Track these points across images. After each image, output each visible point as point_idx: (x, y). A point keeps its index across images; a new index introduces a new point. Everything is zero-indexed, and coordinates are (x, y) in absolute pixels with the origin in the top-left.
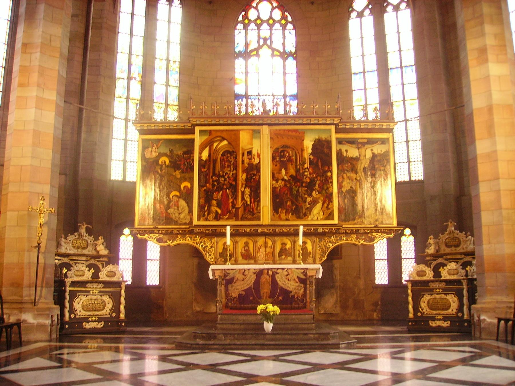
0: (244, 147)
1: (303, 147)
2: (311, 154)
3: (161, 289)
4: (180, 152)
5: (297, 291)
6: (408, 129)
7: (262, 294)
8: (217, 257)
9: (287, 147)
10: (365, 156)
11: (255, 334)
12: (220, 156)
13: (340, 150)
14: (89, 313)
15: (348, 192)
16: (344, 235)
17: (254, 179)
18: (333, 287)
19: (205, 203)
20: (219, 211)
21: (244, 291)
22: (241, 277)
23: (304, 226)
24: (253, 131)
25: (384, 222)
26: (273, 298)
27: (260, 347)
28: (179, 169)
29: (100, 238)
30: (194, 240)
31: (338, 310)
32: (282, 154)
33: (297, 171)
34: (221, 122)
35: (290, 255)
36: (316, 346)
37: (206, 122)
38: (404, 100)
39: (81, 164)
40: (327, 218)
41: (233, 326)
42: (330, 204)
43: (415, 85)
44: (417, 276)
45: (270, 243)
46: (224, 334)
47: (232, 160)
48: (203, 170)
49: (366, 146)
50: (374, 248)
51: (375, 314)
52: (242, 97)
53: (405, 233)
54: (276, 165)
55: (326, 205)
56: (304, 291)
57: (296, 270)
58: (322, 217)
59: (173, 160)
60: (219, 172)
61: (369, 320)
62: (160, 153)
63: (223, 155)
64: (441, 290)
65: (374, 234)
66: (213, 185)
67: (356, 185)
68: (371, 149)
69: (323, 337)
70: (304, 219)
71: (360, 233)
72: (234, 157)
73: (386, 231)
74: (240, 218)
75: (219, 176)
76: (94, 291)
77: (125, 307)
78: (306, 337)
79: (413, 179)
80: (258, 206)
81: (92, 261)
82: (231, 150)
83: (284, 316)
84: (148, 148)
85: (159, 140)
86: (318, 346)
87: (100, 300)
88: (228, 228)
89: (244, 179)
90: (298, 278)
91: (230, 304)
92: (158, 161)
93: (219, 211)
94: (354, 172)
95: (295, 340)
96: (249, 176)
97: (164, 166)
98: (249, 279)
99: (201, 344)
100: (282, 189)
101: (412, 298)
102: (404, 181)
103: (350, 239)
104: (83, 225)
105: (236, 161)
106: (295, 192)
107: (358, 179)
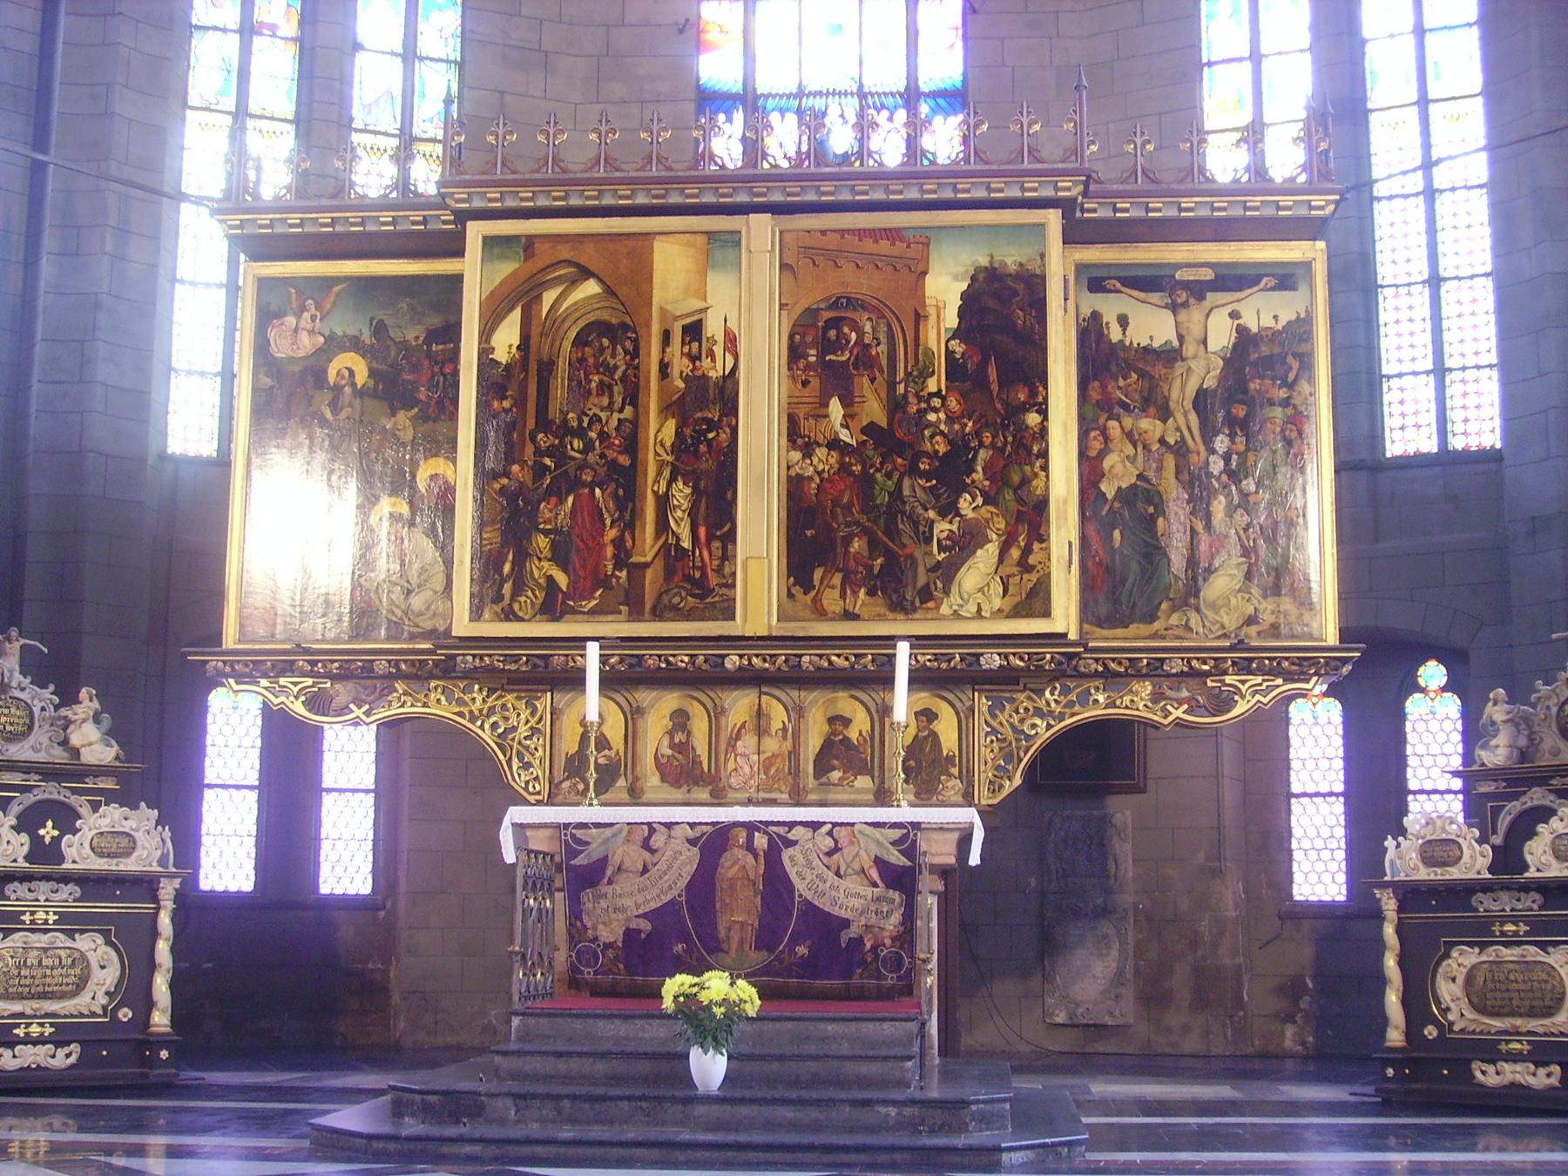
0: (669, 307)
1: (924, 306)
2: (956, 334)
3: (382, 914)
4: (414, 334)
5: (873, 920)
6: (1439, 225)
7: (722, 933)
8: (555, 773)
9: (852, 302)
10: (1205, 342)
11: (642, 1098)
12: (567, 345)
13: (1096, 316)
14: (17, 1007)
15: (1127, 496)
16: (1099, 683)
17: (709, 443)
18: (1104, 912)
19: (504, 545)
20: (562, 580)
21: (644, 916)
22: (633, 856)
23: (918, 641)
24: (710, 235)
25: (1284, 630)
26: (770, 950)
27: (655, 1154)
28: (408, 406)
29: (84, 693)
30: (461, 702)
31: (1126, 1011)
32: (832, 333)
33: (895, 406)
34: (575, 201)
35: (865, 769)
36: (897, 1157)
37: (511, 203)
38: (1423, 102)
39: (36, 387)
40: (1017, 612)
41: (562, 1066)
42: (1036, 546)
43: (1475, 32)
44: (1421, 866)
45: (778, 715)
46: (517, 1097)
47: (620, 361)
48: (496, 404)
50: (1288, 746)
51: (1290, 1031)
52: (728, 104)
53: (1422, 682)
54: (805, 383)
55: (1015, 553)
56: (903, 923)
57: (869, 830)
58: (997, 603)
59: (384, 367)
60: (564, 414)
61: (1264, 1056)
62: (330, 339)
63: (580, 342)
64: (1523, 928)
65: (1228, 679)
66: (539, 471)
67: (1160, 469)
68: (1229, 309)
69: (938, 1117)
70: (917, 616)
71: (1169, 675)
72: (626, 352)
73: (1286, 664)
74: (648, 606)
75: (565, 430)
76: (41, 915)
77: (173, 986)
78: (865, 1116)
79: (1457, 443)
80: (727, 556)
81: (51, 791)
82: (614, 321)
83: (790, 1025)
84: (280, 315)
85: (328, 282)
86: (907, 1156)
87: (63, 953)
88: (593, 649)
89: (668, 444)
90: (879, 862)
91: (588, 973)
92: (325, 372)
93: (562, 580)
94: (1152, 410)
95: (817, 1127)
96: (688, 431)
97: (348, 390)
98: (670, 867)
99: (408, 1139)
100: (828, 486)
101: (1401, 963)
103: (1126, 699)
104: (9, 639)
105: (637, 368)
106: (882, 499)
107: (1172, 442)
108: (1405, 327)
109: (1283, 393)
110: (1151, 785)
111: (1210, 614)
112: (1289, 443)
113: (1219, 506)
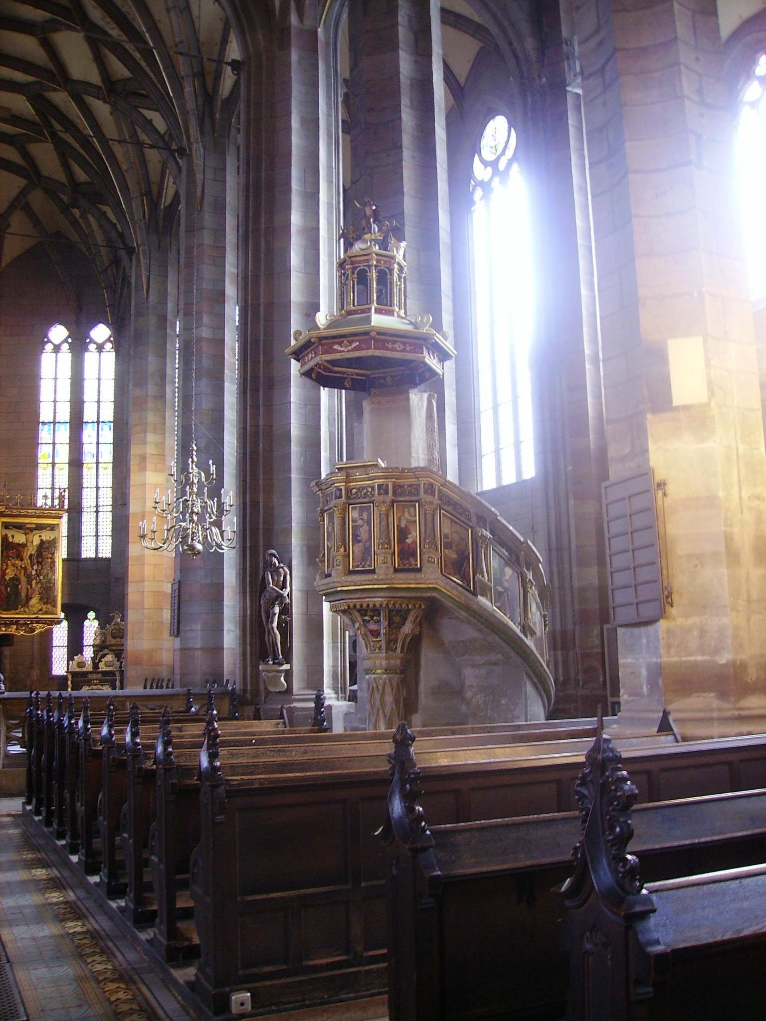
10: (32, 542)
13: (6, 535)
15: (12, 579)
16: (3, 625)
49: (35, 532)
53: (89, 617)
65: (34, 625)
71: (20, 624)
79: (100, 556)
102: (90, 558)
108: (89, 523)
109: (50, 556)
110: (14, 644)
111: (31, 609)
112: (51, 568)
113: (34, 582)
